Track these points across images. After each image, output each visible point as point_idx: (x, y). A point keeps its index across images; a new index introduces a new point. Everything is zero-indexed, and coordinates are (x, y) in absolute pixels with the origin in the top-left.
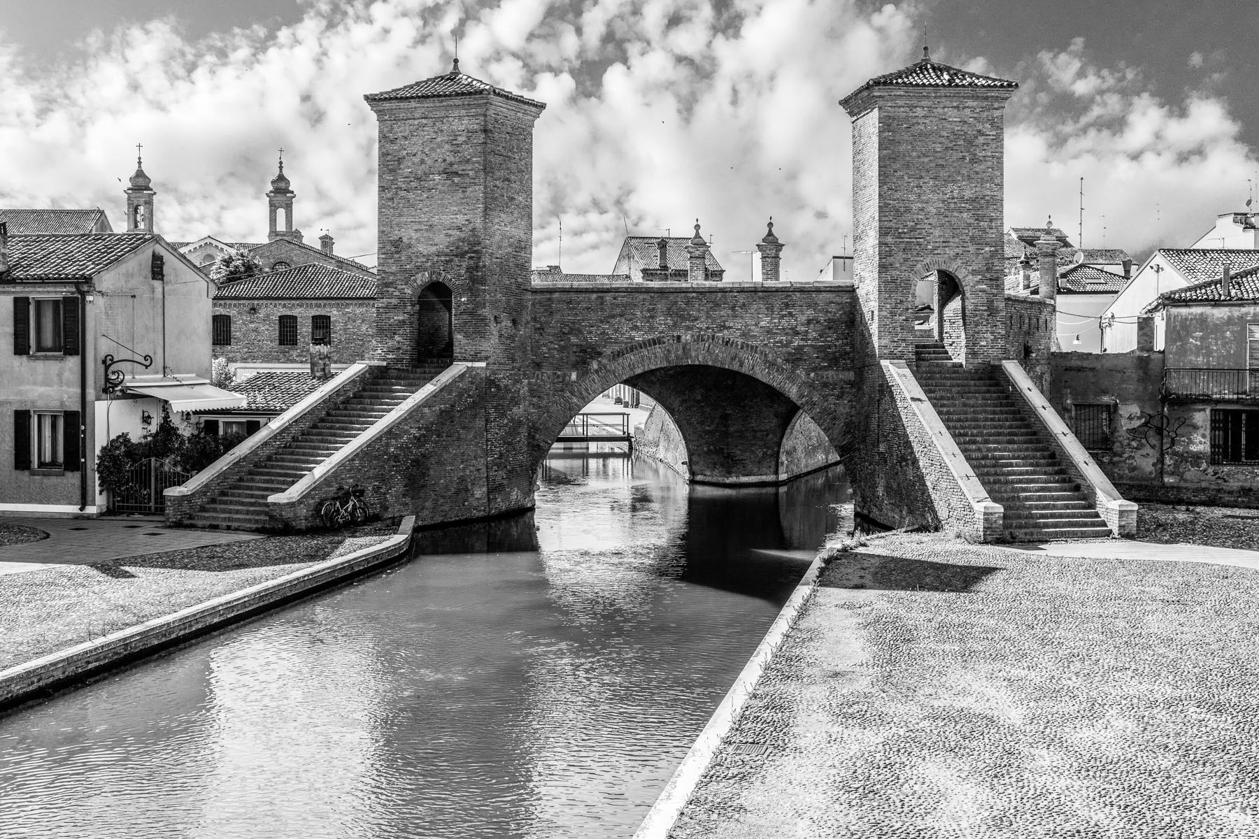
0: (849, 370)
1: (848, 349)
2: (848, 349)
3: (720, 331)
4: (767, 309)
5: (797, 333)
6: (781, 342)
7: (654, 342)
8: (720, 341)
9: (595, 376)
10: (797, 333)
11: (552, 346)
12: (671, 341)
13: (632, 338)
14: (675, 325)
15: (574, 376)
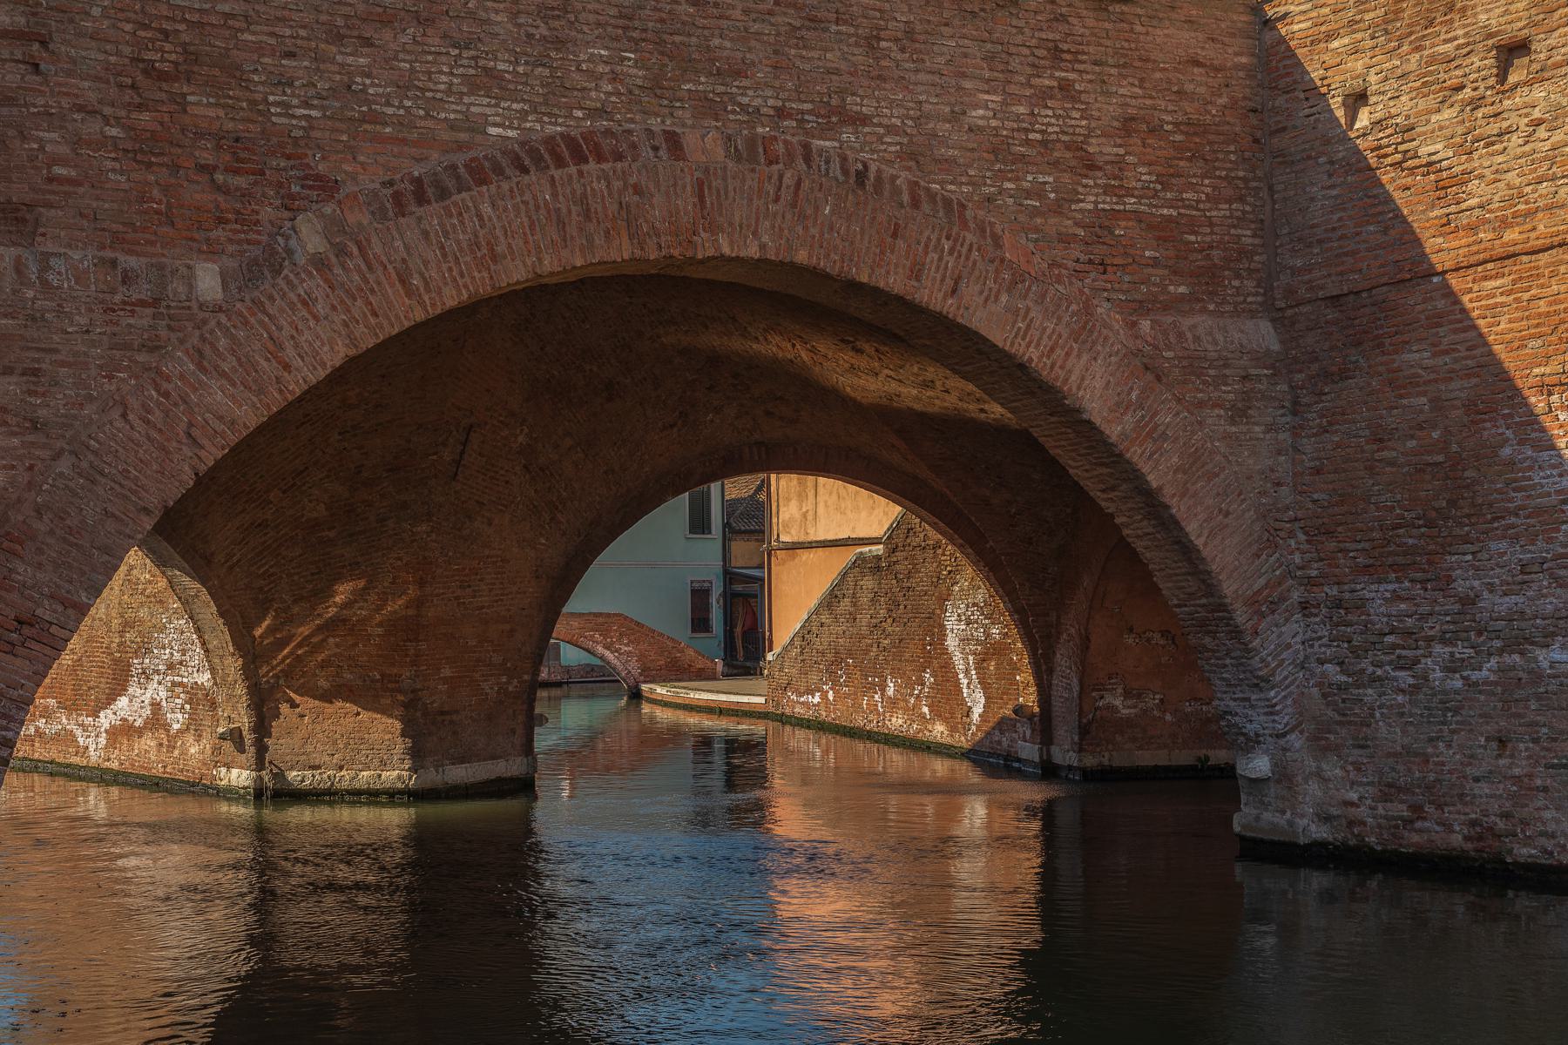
0: (1253, 314)
1: (1247, 237)
2: (1247, 237)
3: (826, 131)
4: (990, 58)
5: (1091, 166)
6: (1038, 192)
7: (577, 150)
8: (836, 166)
9: (314, 285)
10: (1091, 166)
11: (92, 127)
12: (646, 153)
13: (476, 127)
14: (655, 86)
15: (208, 281)
